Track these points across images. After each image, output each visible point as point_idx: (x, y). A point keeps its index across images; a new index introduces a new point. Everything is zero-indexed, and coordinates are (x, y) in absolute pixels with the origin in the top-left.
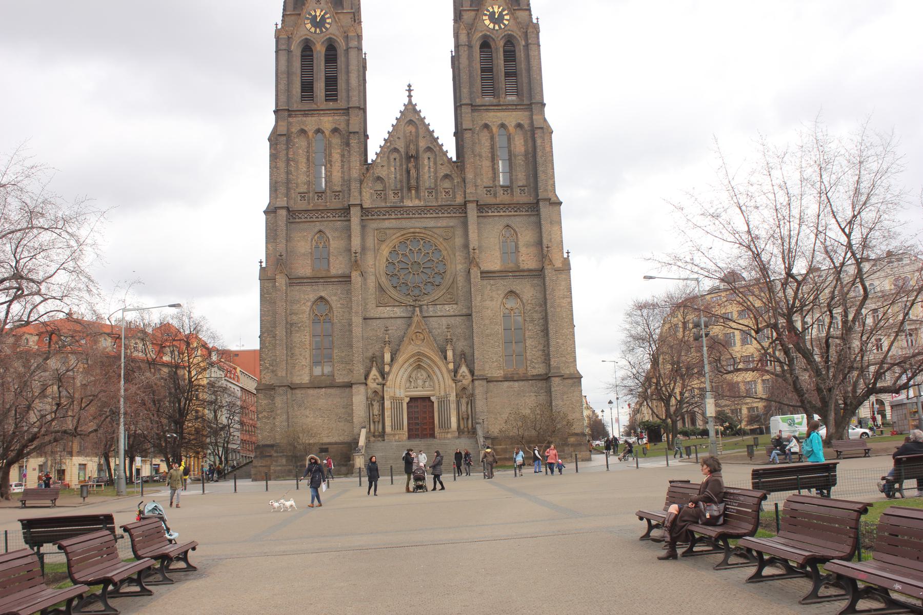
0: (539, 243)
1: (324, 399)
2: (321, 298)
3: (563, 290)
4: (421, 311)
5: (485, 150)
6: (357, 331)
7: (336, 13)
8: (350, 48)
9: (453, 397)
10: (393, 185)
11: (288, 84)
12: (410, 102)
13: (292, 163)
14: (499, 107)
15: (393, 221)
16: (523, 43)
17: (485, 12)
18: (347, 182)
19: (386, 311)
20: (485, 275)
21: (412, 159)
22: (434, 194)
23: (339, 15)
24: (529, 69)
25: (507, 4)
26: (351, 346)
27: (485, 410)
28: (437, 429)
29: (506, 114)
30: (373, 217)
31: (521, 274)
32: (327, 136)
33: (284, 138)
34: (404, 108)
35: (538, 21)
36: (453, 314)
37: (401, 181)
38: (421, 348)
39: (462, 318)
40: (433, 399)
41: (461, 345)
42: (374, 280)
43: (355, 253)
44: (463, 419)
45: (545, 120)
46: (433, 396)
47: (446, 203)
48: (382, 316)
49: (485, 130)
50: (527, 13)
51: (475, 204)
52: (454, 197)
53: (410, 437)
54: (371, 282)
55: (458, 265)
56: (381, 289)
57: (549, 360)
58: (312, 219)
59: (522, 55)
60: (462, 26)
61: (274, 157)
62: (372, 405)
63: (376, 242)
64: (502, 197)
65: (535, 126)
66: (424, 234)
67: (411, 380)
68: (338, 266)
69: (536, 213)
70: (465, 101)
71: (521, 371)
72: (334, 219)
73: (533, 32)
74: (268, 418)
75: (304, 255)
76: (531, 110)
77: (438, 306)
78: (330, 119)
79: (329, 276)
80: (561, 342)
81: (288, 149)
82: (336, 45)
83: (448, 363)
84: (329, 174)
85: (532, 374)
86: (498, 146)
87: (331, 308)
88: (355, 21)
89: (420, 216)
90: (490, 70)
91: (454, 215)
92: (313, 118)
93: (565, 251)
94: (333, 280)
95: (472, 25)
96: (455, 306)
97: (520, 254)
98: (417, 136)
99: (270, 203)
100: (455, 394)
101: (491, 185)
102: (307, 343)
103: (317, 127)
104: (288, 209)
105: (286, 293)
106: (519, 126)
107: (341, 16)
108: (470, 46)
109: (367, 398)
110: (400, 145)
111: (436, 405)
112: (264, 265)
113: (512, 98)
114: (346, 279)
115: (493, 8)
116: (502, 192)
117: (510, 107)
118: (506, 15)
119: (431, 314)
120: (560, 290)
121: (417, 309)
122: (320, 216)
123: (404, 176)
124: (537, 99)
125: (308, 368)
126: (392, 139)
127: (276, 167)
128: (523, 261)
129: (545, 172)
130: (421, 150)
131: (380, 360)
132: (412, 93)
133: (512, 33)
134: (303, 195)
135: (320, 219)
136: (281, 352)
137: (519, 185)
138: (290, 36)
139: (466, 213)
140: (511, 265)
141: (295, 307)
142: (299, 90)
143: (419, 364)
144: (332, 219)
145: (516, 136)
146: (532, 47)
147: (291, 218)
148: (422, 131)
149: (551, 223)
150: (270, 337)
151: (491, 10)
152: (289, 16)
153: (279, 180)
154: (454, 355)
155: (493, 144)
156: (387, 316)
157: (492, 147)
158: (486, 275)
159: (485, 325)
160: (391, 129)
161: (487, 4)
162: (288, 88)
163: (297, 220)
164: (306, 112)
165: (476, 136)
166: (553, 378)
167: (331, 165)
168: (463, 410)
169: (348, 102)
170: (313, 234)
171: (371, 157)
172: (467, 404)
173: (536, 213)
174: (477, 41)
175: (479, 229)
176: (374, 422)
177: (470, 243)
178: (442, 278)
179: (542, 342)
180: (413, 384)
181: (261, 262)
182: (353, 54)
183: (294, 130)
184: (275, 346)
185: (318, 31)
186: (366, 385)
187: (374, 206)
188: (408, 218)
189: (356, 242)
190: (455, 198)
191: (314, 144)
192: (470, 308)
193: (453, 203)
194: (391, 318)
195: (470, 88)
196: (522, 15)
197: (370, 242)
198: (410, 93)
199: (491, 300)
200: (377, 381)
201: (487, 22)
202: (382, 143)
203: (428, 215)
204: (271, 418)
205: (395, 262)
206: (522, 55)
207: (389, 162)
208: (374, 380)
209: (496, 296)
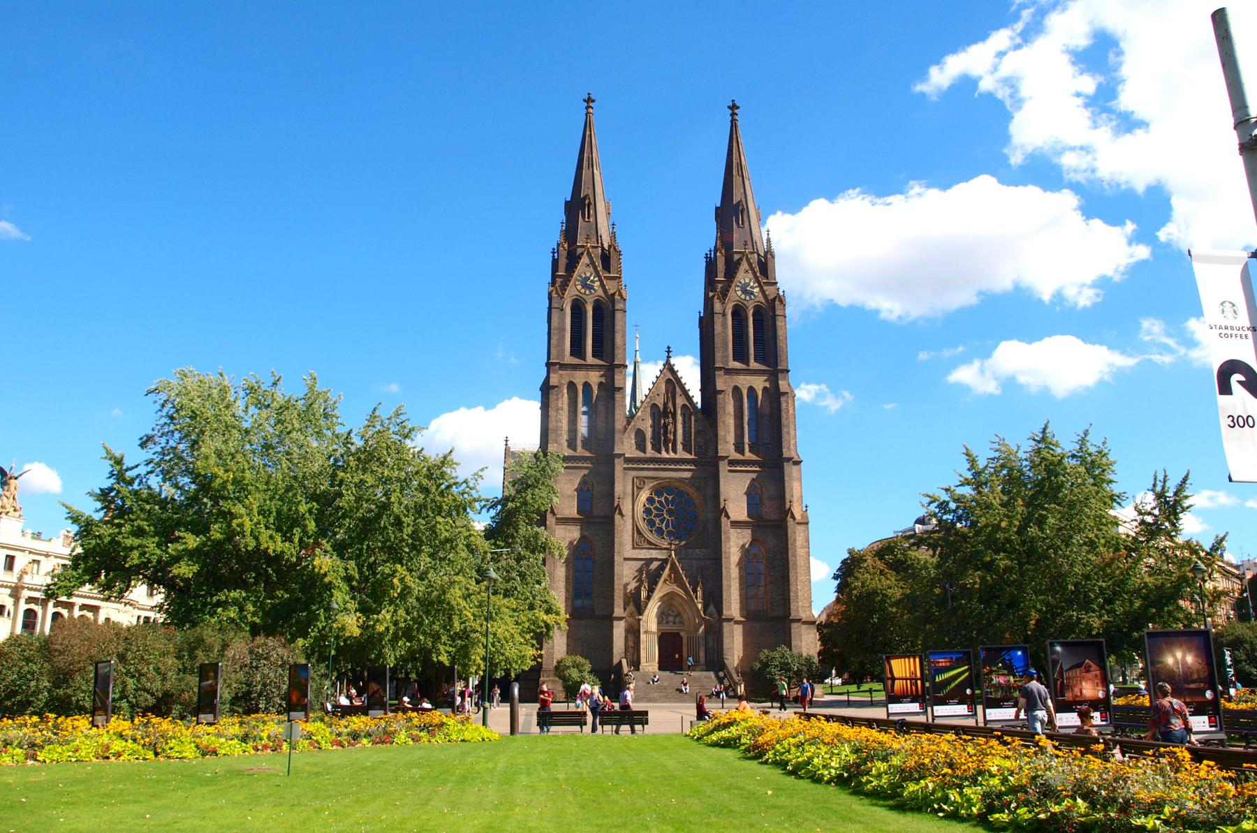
16: (771, 314)
40: (682, 634)
45: (789, 385)
53: (660, 668)
75: (570, 496)
78: (597, 373)
80: (799, 587)
93: (804, 505)
94: (596, 520)
96: (704, 551)
108: (724, 315)
110: (660, 402)
111: (685, 640)
129: (788, 433)
161: (740, 277)
201: (739, 293)
205: (652, 507)
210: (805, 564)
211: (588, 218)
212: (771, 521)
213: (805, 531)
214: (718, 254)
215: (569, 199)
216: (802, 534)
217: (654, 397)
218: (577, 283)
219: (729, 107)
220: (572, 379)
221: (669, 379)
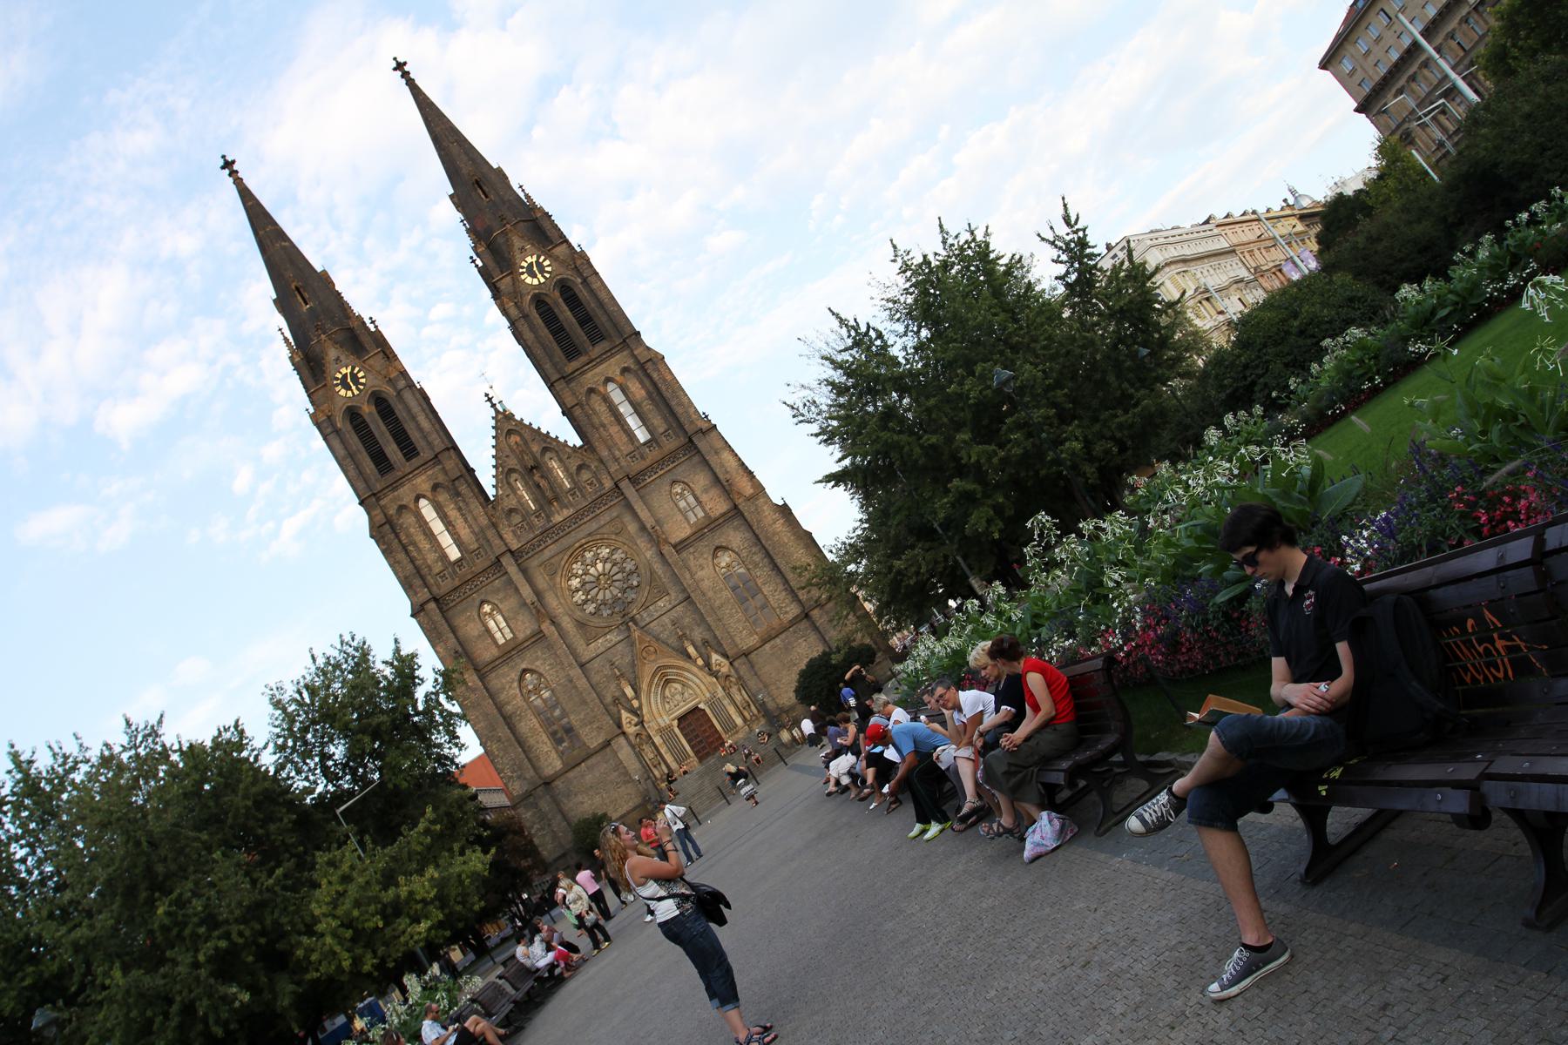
0: (717, 480)
2: (525, 671)
4: (636, 624)
5: (606, 417)
7: (364, 362)
9: (720, 693)
11: (357, 467)
12: (497, 411)
13: (411, 548)
14: (594, 362)
16: (579, 280)
17: (521, 270)
18: (480, 535)
22: (578, 493)
24: (601, 305)
28: (724, 736)
30: (530, 555)
31: (717, 523)
33: (387, 526)
36: (670, 606)
40: (701, 706)
41: (698, 634)
43: (533, 604)
45: (648, 349)
46: (700, 703)
48: (599, 652)
50: (565, 245)
52: (601, 484)
53: (701, 759)
56: (581, 625)
60: (505, 300)
61: (387, 553)
64: (653, 455)
70: (555, 377)
71: (775, 623)
72: (489, 580)
74: (543, 829)
75: (480, 636)
78: (423, 477)
81: (397, 536)
82: (384, 395)
83: (695, 661)
90: (562, 329)
92: (405, 487)
94: (526, 645)
95: (515, 292)
98: (526, 443)
99: (412, 604)
102: (538, 725)
104: (435, 599)
107: (371, 362)
108: (526, 316)
110: (513, 462)
118: (544, 260)
119: (648, 620)
121: (630, 624)
124: (628, 331)
125: (553, 752)
127: (398, 562)
129: (681, 404)
130: (538, 455)
131: (622, 700)
139: (622, 494)
142: (373, 466)
146: (592, 279)
148: (527, 435)
154: (696, 648)
156: (603, 649)
158: (680, 547)
160: (493, 452)
165: (587, 407)
166: (812, 613)
167: (453, 526)
170: (476, 609)
171: (491, 492)
176: (655, 767)
177: (646, 523)
179: (778, 581)
182: (407, 395)
183: (392, 511)
186: (624, 733)
192: (684, 590)
193: (604, 492)
195: (551, 361)
196: (560, 251)
197: (542, 581)
198: (491, 403)
200: (633, 722)
201: (529, 280)
202: (493, 472)
209: (705, 562)
212: (723, 515)
213: (766, 503)
215: (275, 296)
219: (395, 69)
220: (399, 503)
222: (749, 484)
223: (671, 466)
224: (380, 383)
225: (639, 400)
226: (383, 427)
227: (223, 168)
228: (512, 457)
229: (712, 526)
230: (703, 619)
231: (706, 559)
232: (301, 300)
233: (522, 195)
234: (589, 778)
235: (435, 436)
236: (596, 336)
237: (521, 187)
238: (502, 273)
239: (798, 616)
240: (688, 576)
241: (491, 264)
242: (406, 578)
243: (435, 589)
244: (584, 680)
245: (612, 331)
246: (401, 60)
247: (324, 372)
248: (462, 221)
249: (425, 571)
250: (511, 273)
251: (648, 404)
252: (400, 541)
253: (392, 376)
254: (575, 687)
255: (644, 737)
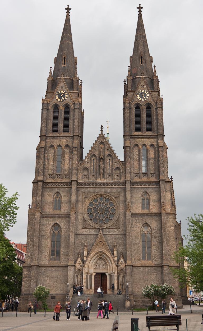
0: (160, 200)
1: (55, 273)
2: (56, 224)
3: (171, 223)
4: (103, 232)
5: (136, 157)
6: (72, 240)
8: (76, 108)
9: (116, 274)
10: (92, 171)
12: (102, 133)
13: (46, 160)
15: (91, 188)
16: (155, 107)
17: (138, 93)
18: (71, 170)
19: (86, 231)
20: (133, 215)
21: (102, 160)
22: (111, 176)
23: (71, 93)
24: (157, 119)
25: (148, 89)
26: (68, 247)
27: (131, 281)
29: (146, 139)
30: (83, 187)
31: (151, 215)
32: (63, 148)
33: (43, 149)
34: (98, 136)
35: (162, 97)
36: (118, 233)
37: (96, 170)
38: (102, 249)
39: (122, 235)
40: (107, 274)
41: (121, 248)
42: (81, 216)
43: (73, 203)
44: (121, 284)
45: (164, 143)
46: (107, 273)
47: (116, 181)
49: (136, 147)
50: (157, 93)
51: (130, 182)
52: (121, 178)
54: (80, 217)
55: (121, 210)
56: (84, 220)
57: (163, 257)
58: (54, 187)
59: (154, 112)
60: (127, 99)
62: (78, 276)
63: (83, 198)
65: (159, 145)
66: (106, 195)
67: (97, 264)
68: (65, 209)
69: (159, 186)
72: (64, 187)
73: (159, 102)
74: (28, 281)
76: (158, 138)
77: (111, 229)
78: (65, 140)
79: (61, 213)
81: (45, 154)
82: (69, 107)
84: (63, 166)
85: (155, 264)
86: (142, 154)
87: (61, 228)
88: (79, 96)
89: (104, 186)
91: (120, 186)
92: (57, 140)
94: (62, 215)
97: (151, 206)
99: (35, 178)
100: (117, 272)
101: (138, 173)
102: (49, 244)
103: (58, 144)
104: (43, 181)
105: (40, 221)
106: (152, 145)
108: (130, 108)
109: (75, 273)
110: (96, 153)
112: (31, 207)
113: (150, 133)
114: (68, 216)
115: (141, 91)
116: (143, 176)
117: (148, 137)
119: (107, 233)
120: (169, 223)
122: (58, 185)
123: (98, 167)
126: (93, 150)
127: (39, 162)
128: (152, 209)
129: (163, 167)
130: (106, 156)
132: (103, 129)
133: (150, 102)
134: (51, 175)
135: (58, 187)
136: (36, 249)
137: (151, 173)
138: (49, 102)
139: (125, 185)
140: (146, 211)
141: (44, 228)
142: (51, 127)
143: (101, 257)
144: (63, 187)
145: (150, 150)
146: (160, 109)
147: (44, 185)
149: (165, 191)
150: (31, 242)
151: (141, 92)
152: (49, 94)
153: (40, 168)
155: (140, 153)
156: (86, 233)
157: (139, 155)
158: (134, 215)
159: (133, 239)
160: (92, 146)
162: (46, 126)
163: (47, 187)
164: (54, 137)
165: (132, 150)
166: (164, 266)
167: (64, 162)
168: (121, 280)
169: (73, 133)
171: (84, 158)
172: (123, 277)
173: (159, 186)
174: (133, 106)
175: (131, 193)
178: (114, 216)
180: (97, 266)
181: (29, 206)
182: (77, 111)
184: (33, 246)
185: (61, 100)
186: (75, 266)
187: (83, 181)
188: (99, 187)
189: (74, 198)
190: (121, 178)
191: (57, 152)
192: (126, 230)
193: (120, 181)
194: (89, 234)
195: (130, 128)
196: (155, 94)
197: (81, 198)
198: (102, 129)
199: (136, 227)
200: (80, 264)
201: (139, 97)
203: (108, 186)
204: (29, 281)
205: (92, 207)
206: (154, 112)
207: (91, 161)
208: (79, 264)
209: (139, 225)
210: (172, 236)
211: (64, 64)
212: (155, 214)
213: (172, 218)
214: (128, 79)
215: (56, 57)
216: (171, 220)
217: (94, 151)
218: (56, 96)
219: (138, 8)
220: (52, 144)
221: (102, 142)
222: (170, 208)
223: (148, 186)
224: (71, 102)
225: (151, 158)
226: (63, 117)
227: (66, 9)
228: (97, 151)
229: (149, 215)
230: (125, 245)
231: (140, 225)
232: (63, 62)
233: (153, 69)
234: (54, 274)
235: (77, 129)
236: (149, 128)
237: (155, 66)
238: (131, 90)
239: (159, 264)
240: (130, 226)
241: (130, 85)
242: (39, 169)
243: (45, 178)
244: (73, 239)
245: (155, 129)
246: (142, 6)
247: (56, 88)
248: (129, 66)
249: (46, 171)
250: (134, 92)
251: (152, 161)
252: (44, 156)
253: (76, 102)
254: (69, 240)
255: (81, 272)
